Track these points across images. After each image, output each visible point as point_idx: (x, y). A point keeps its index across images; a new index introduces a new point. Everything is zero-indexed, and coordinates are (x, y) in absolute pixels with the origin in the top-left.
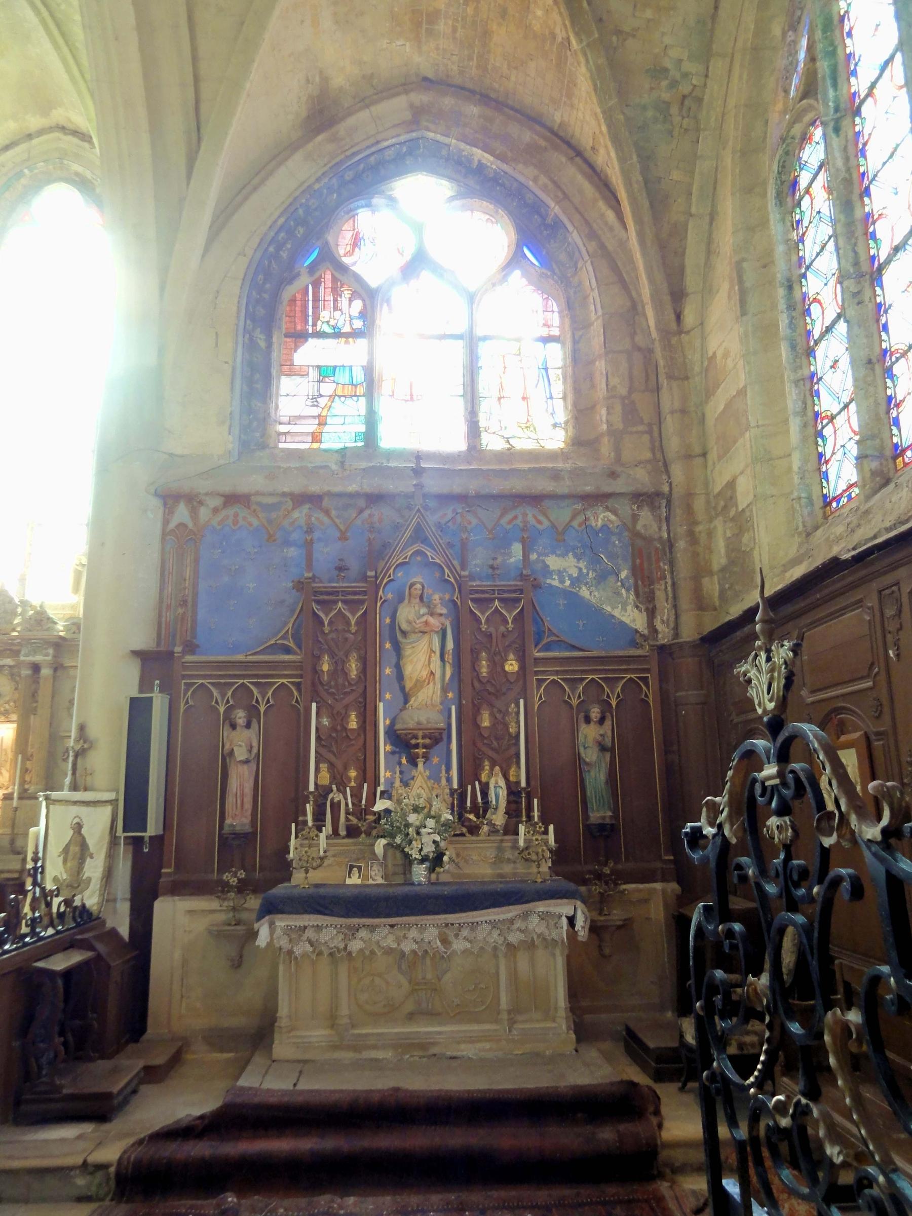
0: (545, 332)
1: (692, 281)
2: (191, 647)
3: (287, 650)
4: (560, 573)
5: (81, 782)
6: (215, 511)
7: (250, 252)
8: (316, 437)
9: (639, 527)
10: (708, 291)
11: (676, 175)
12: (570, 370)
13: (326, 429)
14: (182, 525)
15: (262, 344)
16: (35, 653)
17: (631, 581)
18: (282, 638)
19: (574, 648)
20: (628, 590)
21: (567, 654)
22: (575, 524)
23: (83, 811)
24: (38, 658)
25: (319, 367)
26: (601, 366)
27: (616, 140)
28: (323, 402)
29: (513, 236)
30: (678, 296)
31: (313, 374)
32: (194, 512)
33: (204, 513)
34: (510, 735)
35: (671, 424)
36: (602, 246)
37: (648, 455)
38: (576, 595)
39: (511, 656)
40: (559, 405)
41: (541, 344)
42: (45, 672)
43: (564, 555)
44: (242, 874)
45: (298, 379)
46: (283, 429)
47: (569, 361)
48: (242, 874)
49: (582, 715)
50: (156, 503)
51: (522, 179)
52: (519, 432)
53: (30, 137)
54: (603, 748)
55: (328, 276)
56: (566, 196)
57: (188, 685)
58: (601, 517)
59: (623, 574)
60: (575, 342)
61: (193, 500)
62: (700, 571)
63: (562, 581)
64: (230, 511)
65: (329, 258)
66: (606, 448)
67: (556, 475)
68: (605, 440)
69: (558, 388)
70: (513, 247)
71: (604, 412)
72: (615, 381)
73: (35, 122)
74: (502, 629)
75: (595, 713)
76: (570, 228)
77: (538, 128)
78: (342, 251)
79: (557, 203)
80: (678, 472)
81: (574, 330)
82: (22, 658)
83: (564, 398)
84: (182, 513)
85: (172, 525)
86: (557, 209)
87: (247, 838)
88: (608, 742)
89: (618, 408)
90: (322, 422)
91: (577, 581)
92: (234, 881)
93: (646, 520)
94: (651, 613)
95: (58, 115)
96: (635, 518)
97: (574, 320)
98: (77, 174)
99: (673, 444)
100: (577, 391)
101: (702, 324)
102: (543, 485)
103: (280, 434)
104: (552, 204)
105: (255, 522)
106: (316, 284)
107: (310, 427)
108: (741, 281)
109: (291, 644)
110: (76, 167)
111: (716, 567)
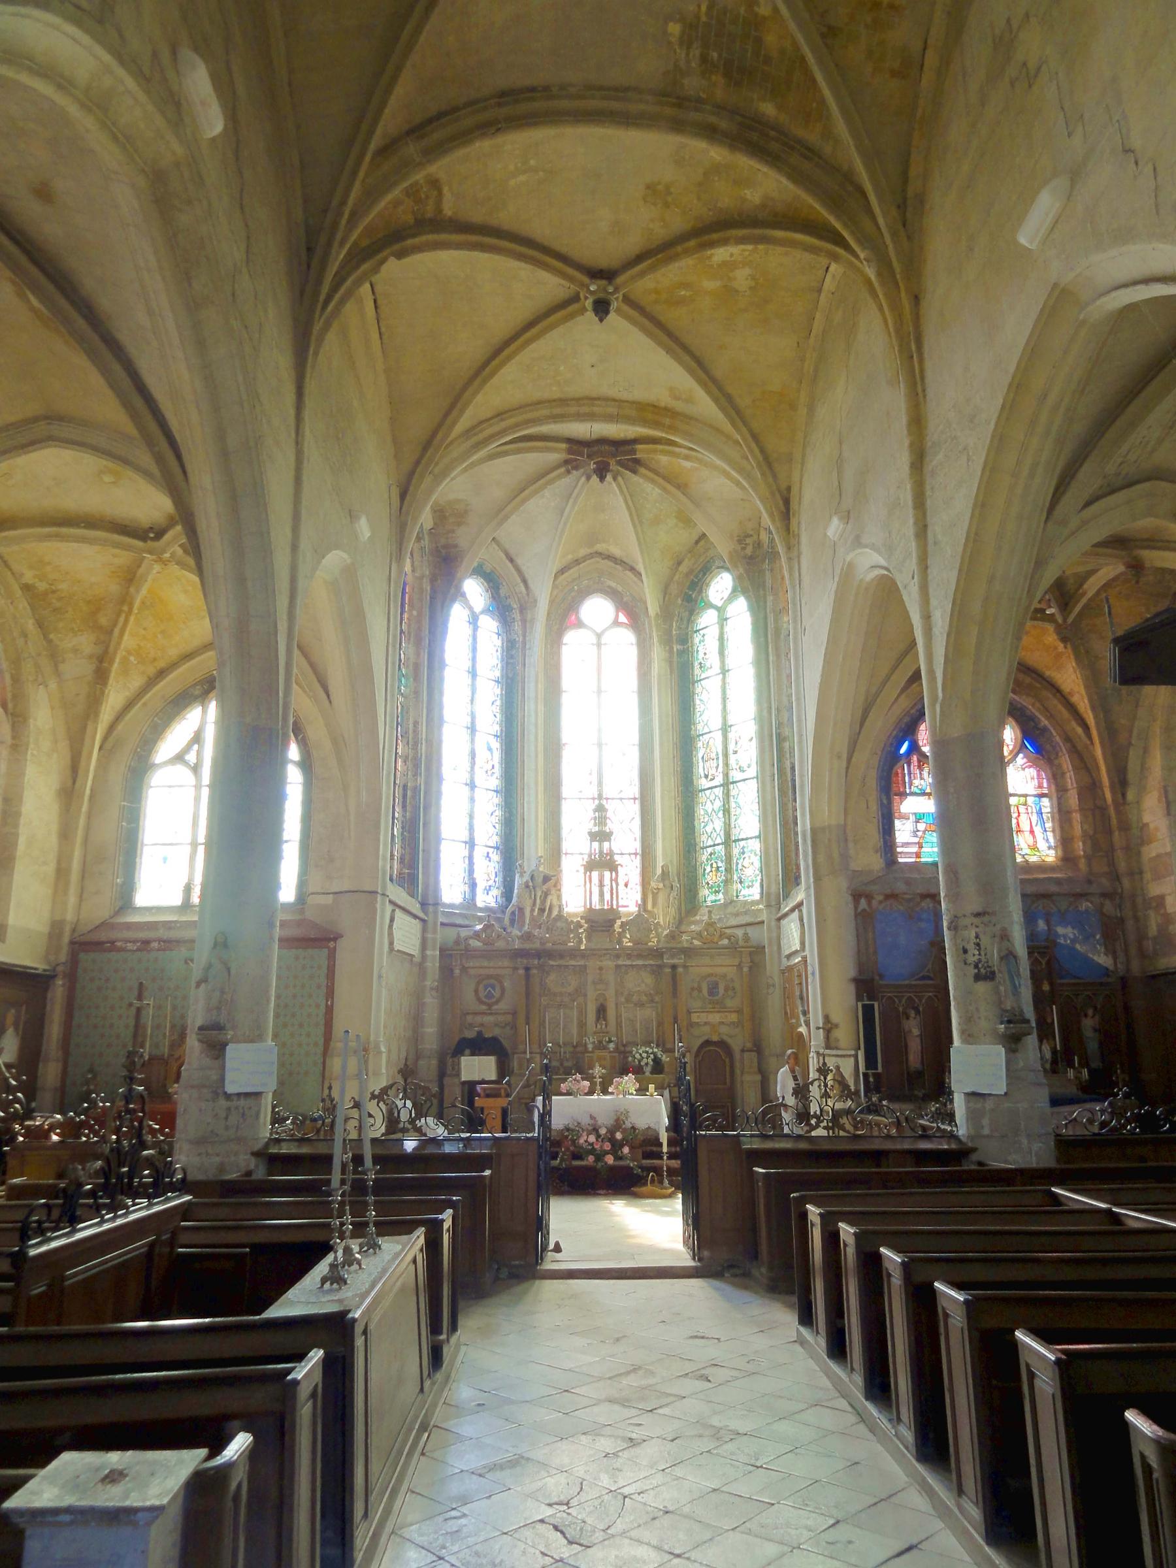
0: (1039, 791)
1: (1131, 777)
2: (881, 976)
3: (929, 978)
4: (1065, 937)
5: (833, 1044)
6: (881, 902)
7: (880, 753)
8: (918, 855)
9: (1104, 910)
10: (1142, 790)
11: (1123, 721)
12: (1057, 816)
13: (923, 850)
14: (864, 910)
15: (885, 802)
16: (673, 956)
17: (1102, 941)
18: (928, 971)
19: (1075, 977)
20: (1100, 945)
21: (1073, 981)
22: (1071, 909)
23: (839, 1059)
24: (675, 961)
25: (915, 814)
26: (1077, 817)
27: (1093, 708)
28: (920, 834)
29: (1019, 735)
30: (1121, 782)
31: (912, 818)
32: (869, 903)
33: (874, 903)
34: (1047, 1023)
35: (1120, 855)
36: (1074, 746)
37: (1106, 869)
38: (1074, 949)
39: (1045, 982)
40: (1050, 835)
41: (1037, 799)
42: (680, 970)
43: (1066, 927)
44: (923, 1091)
45: (905, 821)
46: (899, 850)
47: (1056, 810)
48: (923, 1091)
49: (1083, 1014)
50: (850, 898)
51: (1025, 704)
52: (1029, 851)
53: (577, 562)
54: (1095, 1030)
55: (915, 758)
56: (1051, 715)
57: (883, 997)
58: (1085, 905)
59: (1098, 937)
60: (1059, 799)
61: (869, 897)
62: (1142, 937)
63: (1065, 941)
64: (888, 903)
65: (914, 748)
66: (1082, 864)
67: (1058, 882)
68: (1083, 860)
69: (1049, 825)
70: (1019, 741)
71: (1081, 844)
72: (1086, 827)
73: (583, 552)
74: (1039, 968)
75: (1090, 1012)
76: (1055, 734)
77: (1034, 675)
78: (921, 744)
79: (1047, 718)
80: (1126, 883)
81: (1058, 791)
83: (1053, 831)
84: (863, 903)
85: (859, 910)
86: (1046, 722)
87: (920, 1074)
88: (1097, 1027)
89: (1089, 842)
90: (921, 847)
91: (1074, 941)
92: (920, 1094)
93: (1108, 907)
94: (1115, 959)
95: (599, 547)
96: (1102, 905)
97: (1057, 785)
98: (609, 587)
99: (1122, 866)
100: (1062, 828)
101: (1138, 802)
102: (1054, 888)
103: (900, 853)
104: (1043, 719)
105: (901, 908)
106: (909, 766)
107: (914, 849)
108: (1166, 797)
109: (932, 975)
110: (613, 585)
111: (1150, 935)
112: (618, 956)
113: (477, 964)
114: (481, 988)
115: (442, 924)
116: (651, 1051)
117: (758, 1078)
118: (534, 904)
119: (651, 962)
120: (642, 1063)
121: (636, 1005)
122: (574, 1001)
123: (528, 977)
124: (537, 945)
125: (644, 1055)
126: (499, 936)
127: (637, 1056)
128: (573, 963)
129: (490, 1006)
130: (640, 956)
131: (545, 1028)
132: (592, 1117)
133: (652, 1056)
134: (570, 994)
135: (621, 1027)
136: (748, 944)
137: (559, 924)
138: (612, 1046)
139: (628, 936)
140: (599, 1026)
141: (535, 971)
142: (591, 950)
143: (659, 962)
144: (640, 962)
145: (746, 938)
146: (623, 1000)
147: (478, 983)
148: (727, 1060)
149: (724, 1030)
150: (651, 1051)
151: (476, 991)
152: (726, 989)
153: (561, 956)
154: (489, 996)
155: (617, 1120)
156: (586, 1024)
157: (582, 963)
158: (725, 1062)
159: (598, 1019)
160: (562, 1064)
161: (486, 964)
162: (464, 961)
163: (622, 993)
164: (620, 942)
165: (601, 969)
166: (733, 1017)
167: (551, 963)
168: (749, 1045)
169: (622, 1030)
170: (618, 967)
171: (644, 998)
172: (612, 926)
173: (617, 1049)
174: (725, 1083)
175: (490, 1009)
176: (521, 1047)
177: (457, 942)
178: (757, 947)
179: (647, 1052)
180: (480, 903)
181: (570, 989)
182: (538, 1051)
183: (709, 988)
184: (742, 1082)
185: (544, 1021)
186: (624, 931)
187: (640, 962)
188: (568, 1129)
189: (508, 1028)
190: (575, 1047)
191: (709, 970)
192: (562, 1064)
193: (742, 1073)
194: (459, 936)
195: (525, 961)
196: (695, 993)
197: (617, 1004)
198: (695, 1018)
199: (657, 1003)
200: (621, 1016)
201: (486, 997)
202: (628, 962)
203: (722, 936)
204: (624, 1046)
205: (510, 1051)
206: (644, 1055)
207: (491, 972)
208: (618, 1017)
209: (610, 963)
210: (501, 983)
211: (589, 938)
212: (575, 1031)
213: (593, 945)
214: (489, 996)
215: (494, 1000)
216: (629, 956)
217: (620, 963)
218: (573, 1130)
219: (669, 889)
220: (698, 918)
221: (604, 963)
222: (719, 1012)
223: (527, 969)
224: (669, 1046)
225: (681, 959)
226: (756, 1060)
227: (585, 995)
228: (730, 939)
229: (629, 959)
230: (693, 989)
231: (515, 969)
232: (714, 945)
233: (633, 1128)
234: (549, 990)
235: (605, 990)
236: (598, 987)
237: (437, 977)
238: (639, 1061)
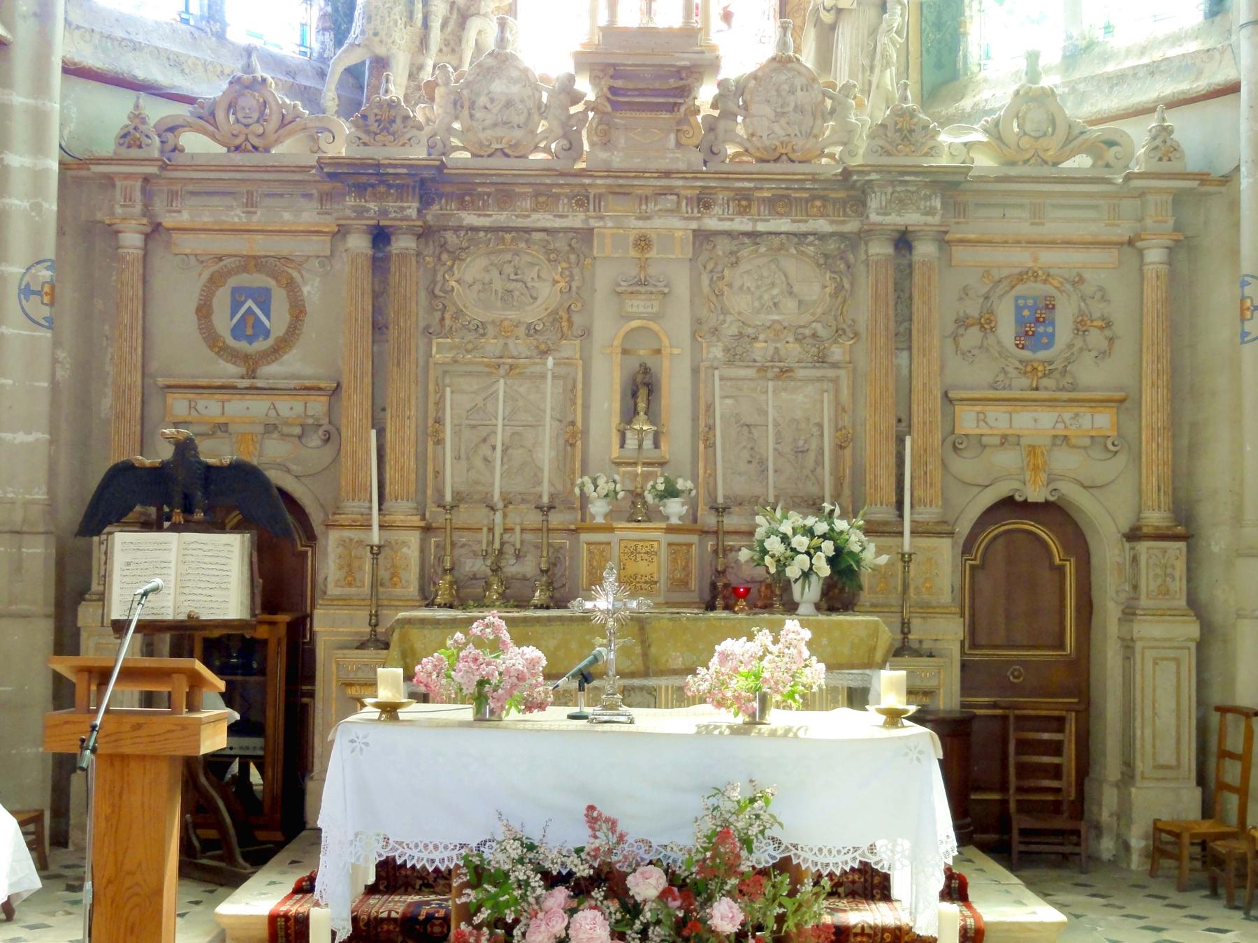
16: (902, 204)
24: (911, 218)
42: (924, 250)
82: (874, 218)
112: (704, 202)
113: (206, 219)
114: (222, 299)
115: (73, 71)
116: (822, 528)
117: (1194, 630)
118: (424, 43)
119: (823, 225)
120: (793, 572)
121: (762, 369)
122: (545, 353)
123: (380, 264)
124: (418, 153)
125: (801, 542)
126: (283, 123)
127: (774, 545)
128: (543, 219)
129: (251, 364)
130: (779, 203)
131: (439, 442)
132: (593, 817)
133: (828, 547)
134: (531, 331)
135: (710, 446)
136: (1175, 166)
137: (498, 87)
138: (675, 509)
139: (741, 131)
140: (631, 443)
141: (403, 244)
142: (610, 173)
143: (852, 226)
144: (783, 224)
145: (1164, 145)
146: (717, 352)
147: (215, 281)
148: (1070, 568)
149: (1065, 461)
150: (822, 528)
151: (204, 311)
152: (1081, 327)
153: (504, 193)
154: (248, 328)
155: (722, 835)
156: (585, 432)
157: (576, 220)
158: (1061, 569)
159: (629, 415)
160: (496, 570)
161: (237, 216)
162: (159, 206)
163: (715, 331)
164: (712, 153)
165: (643, 243)
166: (1103, 421)
167: (470, 219)
168: (1156, 518)
169: (711, 462)
170: (703, 237)
171: (792, 350)
172: (685, 92)
173: (692, 525)
174: (1061, 646)
175: (252, 374)
176: (352, 507)
177: (131, 138)
178: (1203, 178)
179: (809, 532)
180: (237, 35)
181: (533, 314)
182: (416, 520)
183: (1020, 320)
184: (1128, 646)
185: (439, 421)
186: (728, 115)
187: (783, 224)
188: (479, 875)
189: (315, 440)
190: (546, 510)
191: (1022, 258)
192: (496, 570)
193: (1129, 613)
194: (138, 117)
195: (373, 206)
196: (972, 337)
197: (695, 371)
198: (967, 420)
199: (835, 365)
200: (710, 407)
201: (237, 332)
202: (742, 224)
203: (1073, 140)
204: (720, 510)
205: (316, 518)
206: (801, 542)
207: (260, 246)
208: (701, 411)
209: (675, 222)
210: (291, 287)
211: (605, 139)
212: (546, 455)
213: (617, 160)
214: (248, 328)
215: (261, 345)
216: (744, 201)
217: (711, 223)
218: (500, 879)
219: (872, 13)
220: (967, 104)
221: (658, 222)
222: (1051, 403)
223: (380, 236)
224: (884, 513)
225: (930, 212)
226: (1180, 567)
227: (586, 333)
228: (1097, 156)
229: (743, 211)
230: (963, 323)
231: (341, 232)
232: (1046, 171)
233: (784, 865)
234: (458, 314)
235: (655, 317)
236: (636, 305)
237: (50, 252)
238: (782, 564)
